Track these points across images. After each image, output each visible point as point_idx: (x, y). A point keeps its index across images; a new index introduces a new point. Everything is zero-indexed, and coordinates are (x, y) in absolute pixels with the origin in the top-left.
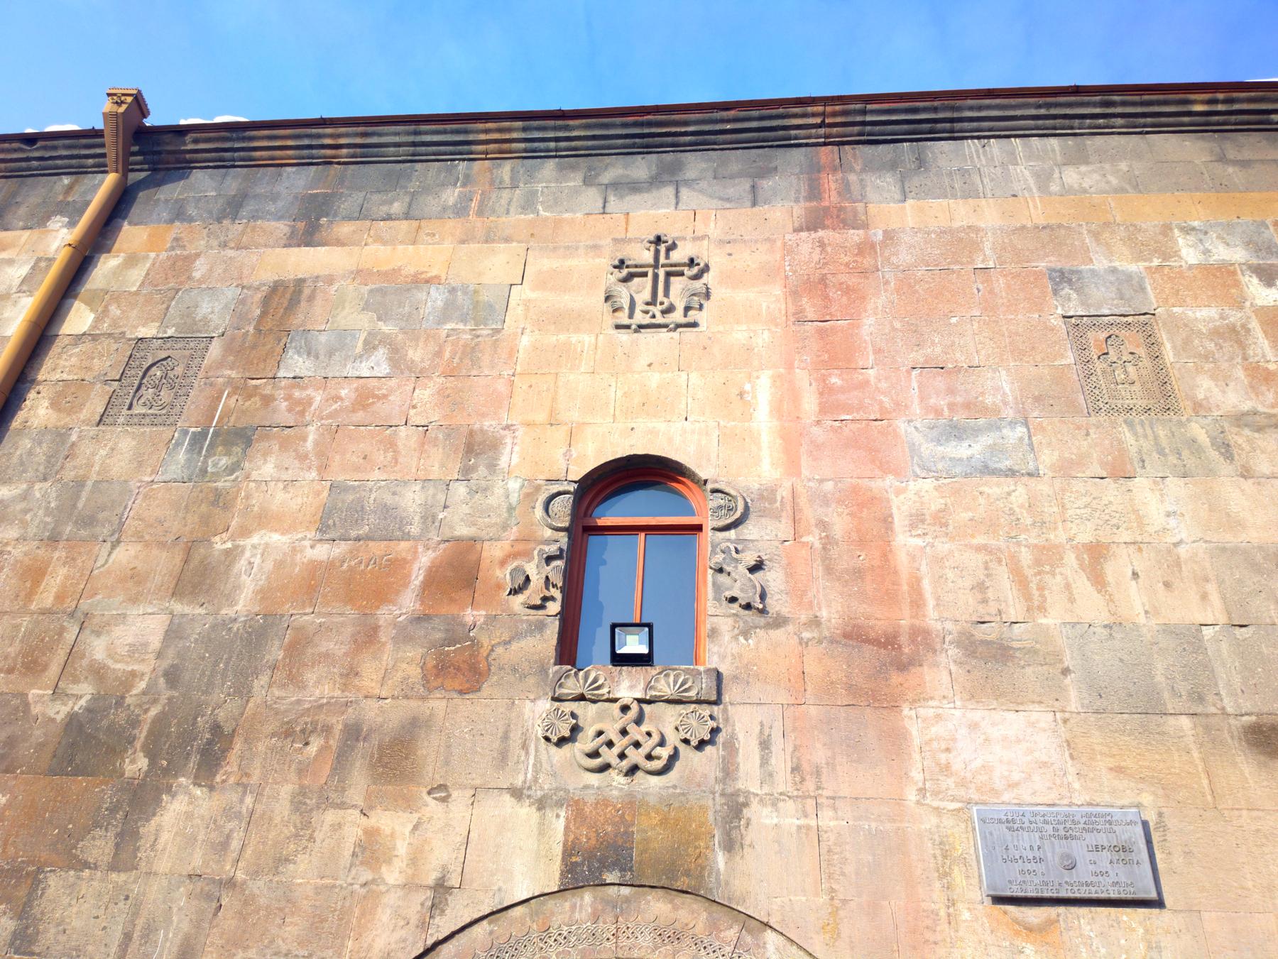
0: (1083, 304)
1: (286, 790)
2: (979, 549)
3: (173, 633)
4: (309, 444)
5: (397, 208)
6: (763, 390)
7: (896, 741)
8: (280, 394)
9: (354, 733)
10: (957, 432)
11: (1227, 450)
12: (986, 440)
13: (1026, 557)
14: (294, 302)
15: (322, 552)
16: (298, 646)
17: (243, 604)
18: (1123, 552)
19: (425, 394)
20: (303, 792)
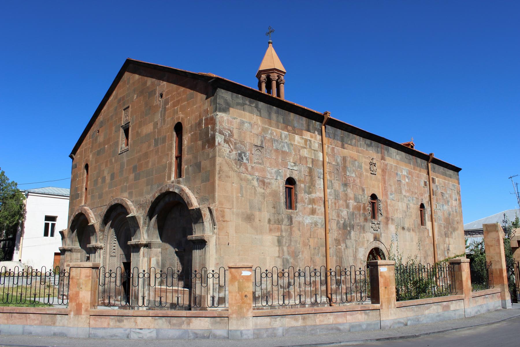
0: (398, 179)
1: (358, 231)
2: (392, 209)
3: (347, 213)
6: (380, 185)
7: (388, 227)
8: (348, 178)
9: (361, 226)
10: (391, 194)
12: (393, 196)
14: (346, 161)
17: (351, 210)
19: (358, 181)
20: (359, 232)
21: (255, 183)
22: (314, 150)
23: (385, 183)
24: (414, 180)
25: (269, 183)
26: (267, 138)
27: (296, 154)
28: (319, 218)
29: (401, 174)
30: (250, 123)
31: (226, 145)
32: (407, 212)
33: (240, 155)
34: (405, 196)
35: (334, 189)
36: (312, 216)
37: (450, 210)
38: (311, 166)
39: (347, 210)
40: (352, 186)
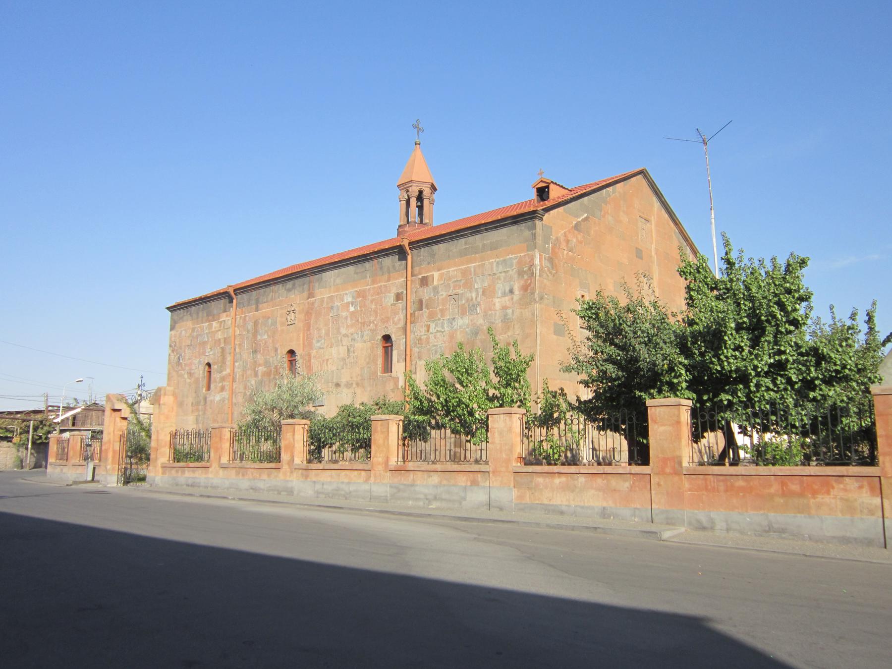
4: (262, 352)
5: (265, 300)
6: (301, 335)
10: (318, 341)
11: (341, 340)
13: (322, 361)
15: (265, 369)
16: (265, 383)
17: (260, 377)
18: (330, 360)
19: (271, 341)
21: (186, 376)
22: (227, 329)
23: (309, 329)
24: (368, 302)
25: (194, 373)
26: (195, 336)
27: (212, 340)
28: (225, 394)
29: (339, 304)
30: (185, 330)
31: (172, 354)
33: (179, 358)
34: (346, 335)
35: (242, 360)
36: (221, 393)
38: (223, 346)
39: (256, 379)
40: (263, 349)
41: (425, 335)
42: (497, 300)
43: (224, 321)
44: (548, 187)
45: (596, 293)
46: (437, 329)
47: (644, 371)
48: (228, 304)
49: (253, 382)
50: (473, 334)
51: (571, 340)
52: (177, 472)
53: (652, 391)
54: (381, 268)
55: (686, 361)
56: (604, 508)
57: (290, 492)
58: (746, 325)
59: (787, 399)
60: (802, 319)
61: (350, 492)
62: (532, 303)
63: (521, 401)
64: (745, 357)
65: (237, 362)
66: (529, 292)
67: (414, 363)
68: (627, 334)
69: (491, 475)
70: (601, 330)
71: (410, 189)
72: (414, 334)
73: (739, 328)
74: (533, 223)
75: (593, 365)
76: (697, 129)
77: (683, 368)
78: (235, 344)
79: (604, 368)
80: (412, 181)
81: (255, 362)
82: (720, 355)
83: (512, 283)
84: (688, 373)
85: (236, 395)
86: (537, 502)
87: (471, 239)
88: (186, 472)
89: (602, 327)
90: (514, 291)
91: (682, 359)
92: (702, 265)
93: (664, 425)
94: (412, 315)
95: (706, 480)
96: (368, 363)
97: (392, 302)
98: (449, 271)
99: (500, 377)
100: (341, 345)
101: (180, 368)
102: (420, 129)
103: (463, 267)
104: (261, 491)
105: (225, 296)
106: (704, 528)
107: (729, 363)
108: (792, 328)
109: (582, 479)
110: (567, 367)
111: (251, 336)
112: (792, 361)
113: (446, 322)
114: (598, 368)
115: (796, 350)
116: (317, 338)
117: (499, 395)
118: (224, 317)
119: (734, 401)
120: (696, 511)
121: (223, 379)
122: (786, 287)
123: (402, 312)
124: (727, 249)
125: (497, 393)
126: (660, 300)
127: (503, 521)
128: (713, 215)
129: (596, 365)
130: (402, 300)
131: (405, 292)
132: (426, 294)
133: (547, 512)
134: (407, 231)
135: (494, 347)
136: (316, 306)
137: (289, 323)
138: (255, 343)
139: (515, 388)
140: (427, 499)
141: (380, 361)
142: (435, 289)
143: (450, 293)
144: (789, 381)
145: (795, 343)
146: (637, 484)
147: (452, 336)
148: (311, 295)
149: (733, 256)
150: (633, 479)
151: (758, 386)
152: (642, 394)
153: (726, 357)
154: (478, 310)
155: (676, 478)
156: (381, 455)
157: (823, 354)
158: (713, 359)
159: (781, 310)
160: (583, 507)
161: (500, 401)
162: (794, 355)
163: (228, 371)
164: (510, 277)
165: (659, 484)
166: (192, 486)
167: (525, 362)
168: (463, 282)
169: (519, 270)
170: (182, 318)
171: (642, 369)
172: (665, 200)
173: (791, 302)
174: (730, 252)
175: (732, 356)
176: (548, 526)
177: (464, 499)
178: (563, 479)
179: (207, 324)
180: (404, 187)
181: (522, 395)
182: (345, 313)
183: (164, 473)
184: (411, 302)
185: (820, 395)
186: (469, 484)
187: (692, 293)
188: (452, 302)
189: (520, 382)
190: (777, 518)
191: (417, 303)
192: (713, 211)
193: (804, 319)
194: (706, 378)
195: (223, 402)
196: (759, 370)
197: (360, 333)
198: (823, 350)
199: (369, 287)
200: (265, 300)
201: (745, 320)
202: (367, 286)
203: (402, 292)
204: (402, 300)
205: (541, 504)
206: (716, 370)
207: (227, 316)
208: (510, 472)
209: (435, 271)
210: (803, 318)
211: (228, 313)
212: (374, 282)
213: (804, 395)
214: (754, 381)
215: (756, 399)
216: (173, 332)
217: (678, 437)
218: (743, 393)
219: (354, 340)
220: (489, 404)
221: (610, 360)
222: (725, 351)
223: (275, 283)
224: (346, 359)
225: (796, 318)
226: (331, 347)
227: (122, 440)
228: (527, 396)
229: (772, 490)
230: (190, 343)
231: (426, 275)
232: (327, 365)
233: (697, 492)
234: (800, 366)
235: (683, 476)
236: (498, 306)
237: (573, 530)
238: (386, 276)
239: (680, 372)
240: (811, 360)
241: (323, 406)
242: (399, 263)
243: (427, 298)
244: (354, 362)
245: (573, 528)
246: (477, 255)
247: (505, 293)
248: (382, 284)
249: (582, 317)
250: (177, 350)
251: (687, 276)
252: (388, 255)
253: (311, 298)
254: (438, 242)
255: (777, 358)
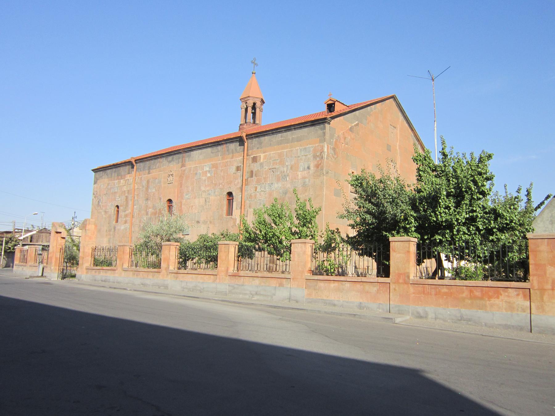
5: (154, 167)
6: (176, 190)
10: (187, 194)
11: (201, 194)
15: (153, 211)
17: (149, 216)
18: (194, 206)
21: (103, 213)
22: (130, 184)
23: (181, 187)
25: (108, 212)
28: (128, 225)
31: (95, 199)
32: (205, 205)
33: (99, 202)
34: (204, 191)
36: (124, 225)
37: (289, 185)
38: (127, 195)
39: (146, 216)
41: (254, 193)
42: (299, 173)
43: (128, 179)
44: (334, 104)
45: (361, 170)
46: (261, 189)
47: (389, 220)
48: (131, 169)
49: (145, 219)
50: (283, 193)
51: (345, 198)
52: (96, 272)
53: (393, 232)
54: (228, 150)
55: (415, 214)
56: (360, 303)
57: (166, 287)
58: (453, 193)
59: (476, 240)
60: (487, 191)
61: (204, 288)
62: (322, 176)
63: (312, 236)
64: (451, 213)
65: (135, 205)
66: (320, 168)
67: (246, 210)
68: (380, 196)
69: (291, 280)
70: (363, 194)
71: (248, 102)
72: (247, 192)
73: (448, 195)
74: (324, 126)
75: (357, 215)
76: (429, 71)
77: (413, 219)
78: (134, 194)
79: (364, 217)
80: (249, 96)
81: (147, 206)
82: (436, 211)
83: (309, 162)
84: (416, 222)
85: (134, 226)
86: (319, 298)
87: (285, 134)
88: (101, 272)
89: (364, 191)
90: (310, 168)
91: (412, 213)
92: (428, 156)
93: (399, 253)
94: (246, 180)
95: (424, 288)
96: (218, 209)
97: (234, 172)
98: (270, 154)
99: (300, 220)
100: (201, 197)
101: (99, 208)
102: (256, 64)
103: (279, 151)
104: (148, 286)
105: (129, 164)
106: (421, 317)
107: (441, 216)
108: (481, 196)
109: (348, 285)
110: (341, 215)
111: (145, 189)
112: (480, 216)
113: (267, 185)
114: (360, 216)
115: (483, 210)
116: (186, 192)
117: (298, 231)
118: (128, 177)
119: (443, 240)
120: (417, 306)
121: (126, 216)
122: (478, 171)
123: (240, 177)
124: (443, 146)
125: (297, 230)
126: (401, 176)
127: (298, 309)
128: (436, 125)
129: (359, 214)
130: (240, 171)
131: (242, 166)
132: (255, 167)
133: (325, 304)
134: (245, 128)
135: (297, 201)
136: (186, 172)
137: (169, 182)
138: (147, 194)
139: (308, 228)
140: (251, 294)
141: (225, 208)
142: (261, 164)
143: (271, 167)
144: (478, 229)
145: (482, 205)
146: (381, 289)
147: (270, 194)
148: (183, 165)
149: (447, 151)
150: (379, 286)
151: (458, 231)
152: (387, 234)
153: (440, 213)
154: (288, 178)
155: (406, 286)
156: (224, 266)
157: (499, 213)
158: (432, 214)
159: (475, 185)
160: (347, 302)
161: (299, 235)
162: (481, 213)
163: (130, 211)
164: (308, 159)
165: (395, 289)
166: (105, 281)
167: (315, 212)
168: (278, 161)
169: (314, 154)
170: (101, 177)
171: (387, 219)
172: (406, 115)
173: (481, 180)
174: (445, 148)
175: (443, 212)
176: (325, 312)
177: (274, 295)
178: (336, 284)
179: (117, 181)
180: (244, 100)
181: (313, 232)
182: (204, 178)
183: (87, 273)
184: (246, 172)
185: (496, 238)
186: (278, 285)
187: (420, 173)
188: (271, 173)
189: (312, 224)
190: (466, 312)
191: (250, 173)
192: (436, 122)
193: (489, 191)
194: (427, 225)
195: (126, 230)
196: (460, 221)
197: (213, 190)
198: (499, 211)
199: (220, 162)
200: (154, 167)
201: (453, 190)
202: (219, 161)
203: (241, 166)
204: (240, 171)
205: (322, 299)
206: (433, 220)
207: (130, 177)
208: (303, 279)
209: (262, 154)
210: (488, 190)
211: (131, 175)
212: (223, 159)
213: (486, 238)
214: (456, 228)
215: (457, 239)
216: (95, 185)
217: (408, 261)
218: (449, 235)
219: (209, 194)
220: (292, 237)
221: (368, 212)
222: (439, 209)
223: (161, 157)
224: (204, 206)
225: (484, 190)
226: (195, 198)
227: (62, 251)
228: (316, 233)
229: (464, 295)
230: (106, 192)
231: (256, 156)
232: (192, 209)
233: (418, 294)
234: (485, 220)
235: (410, 285)
236: (300, 177)
237: (341, 316)
238: (231, 156)
239: (411, 221)
240: (492, 217)
241: (188, 235)
242: (239, 147)
243: (256, 170)
244: (209, 209)
245: (341, 314)
246: (288, 144)
247: (305, 168)
248: (228, 160)
249: (352, 185)
250: (98, 197)
251: (418, 162)
252: (232, 142)
253: (183, 167)
254: (264, 135)
255: (471, 214)
